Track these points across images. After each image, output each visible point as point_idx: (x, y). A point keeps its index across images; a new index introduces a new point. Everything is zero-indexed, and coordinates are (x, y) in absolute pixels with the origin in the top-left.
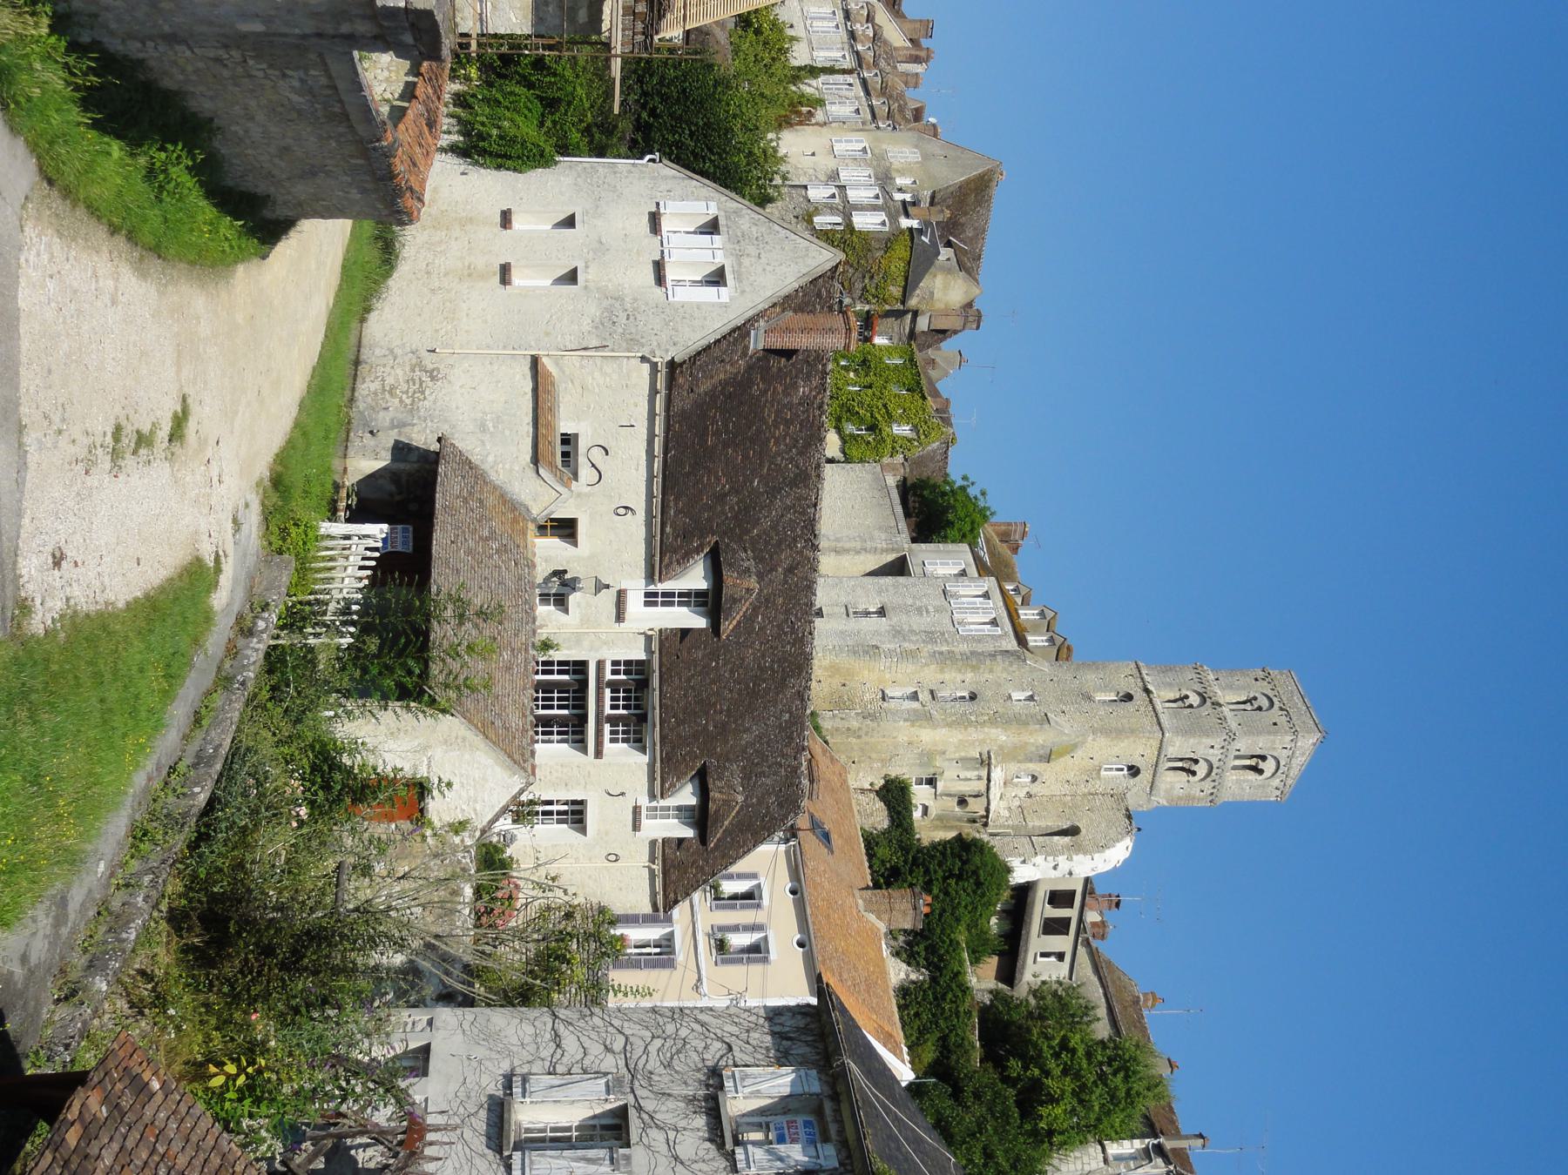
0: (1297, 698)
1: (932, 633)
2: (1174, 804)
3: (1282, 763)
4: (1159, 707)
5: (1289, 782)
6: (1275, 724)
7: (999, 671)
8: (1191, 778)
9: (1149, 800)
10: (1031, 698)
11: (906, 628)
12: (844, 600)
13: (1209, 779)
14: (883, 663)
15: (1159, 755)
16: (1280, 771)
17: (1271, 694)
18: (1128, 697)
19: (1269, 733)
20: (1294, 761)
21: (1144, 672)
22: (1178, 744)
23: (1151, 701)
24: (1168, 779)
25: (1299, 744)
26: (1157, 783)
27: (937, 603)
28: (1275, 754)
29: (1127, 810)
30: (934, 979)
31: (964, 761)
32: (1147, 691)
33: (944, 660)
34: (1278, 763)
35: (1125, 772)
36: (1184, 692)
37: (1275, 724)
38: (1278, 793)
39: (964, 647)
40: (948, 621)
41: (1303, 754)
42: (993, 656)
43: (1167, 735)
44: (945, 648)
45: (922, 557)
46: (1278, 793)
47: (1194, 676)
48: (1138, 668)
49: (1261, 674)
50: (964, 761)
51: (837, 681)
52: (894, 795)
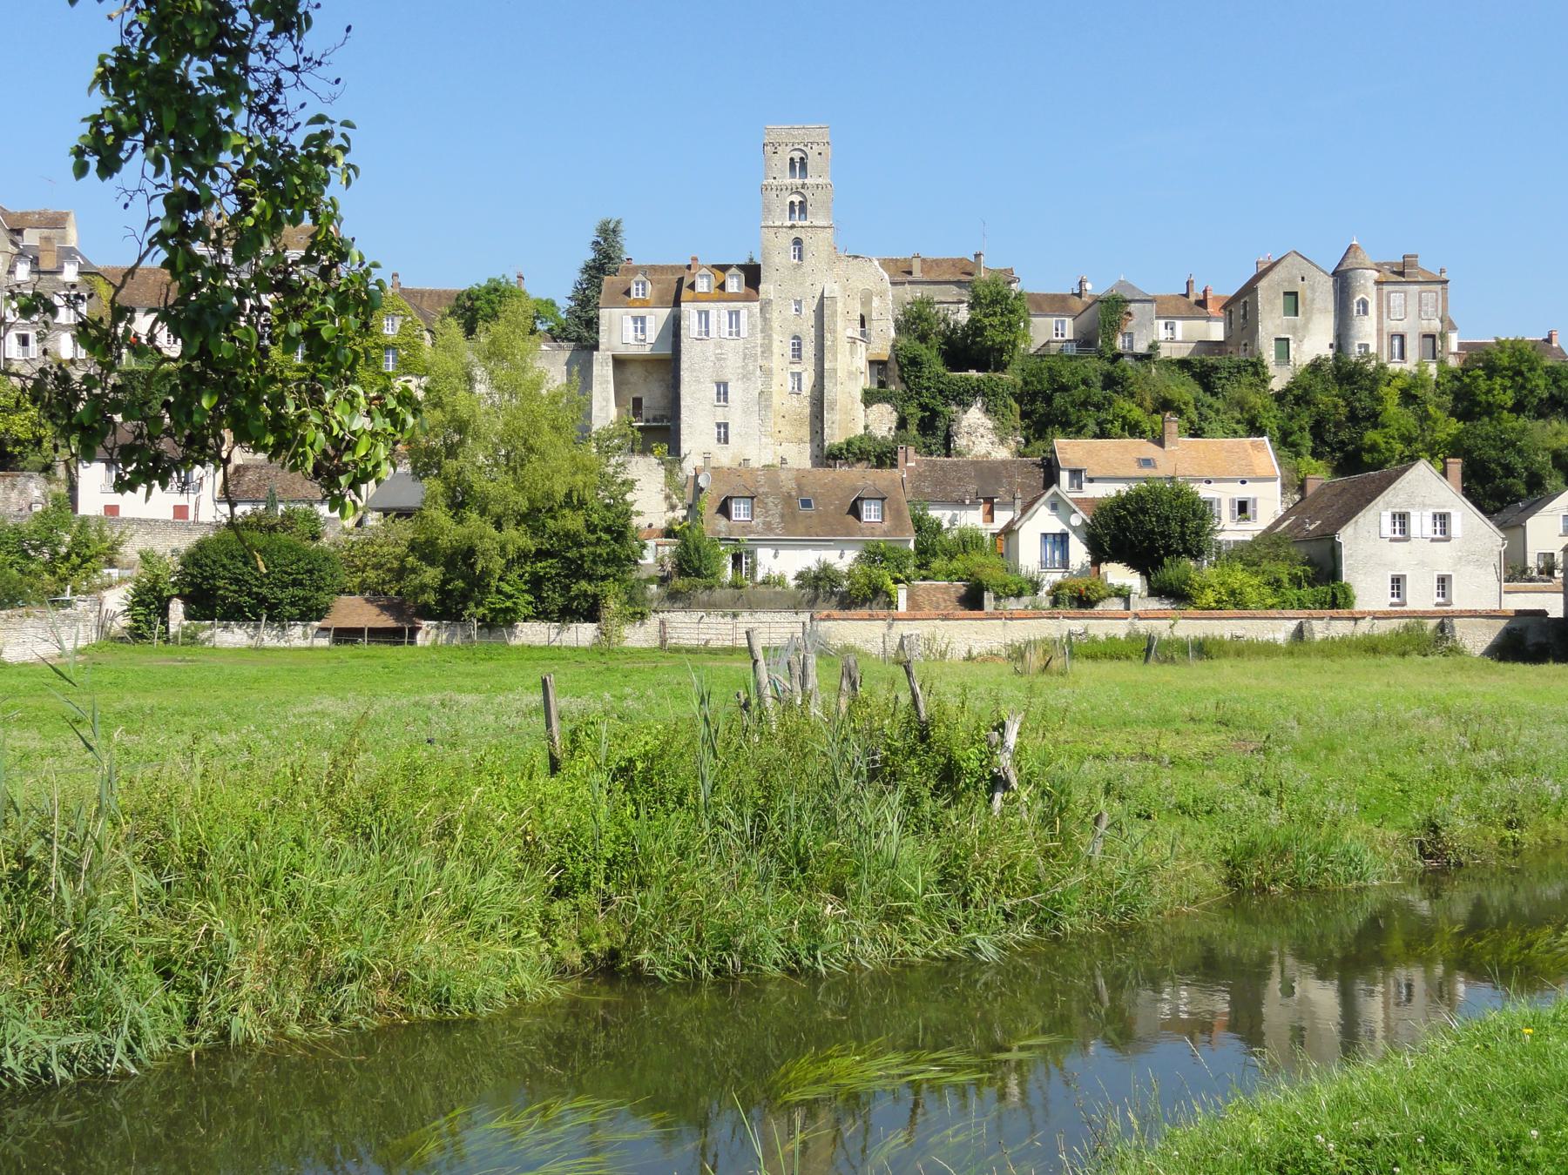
1: (745, 355)
4: (807, 223)
7: (775, 316)
10: (798, 303)
11: (740, 371)
12: (708, 407)
14: (775, 388)
17: (790, 148)
18: (798, 242)
21: (771, 224)
27: (712, 347)
30: (984, 395)
31: (852, 353)
32: (792, 227)
33: (767, 350)
39: (759, 336)
40: (732, 343)
42: (765, 320)
44: (759, 350)
45: (616, 341)
47: (774, 192)
50: (852, 353)
51: (780, 420)
52: (869, 399)
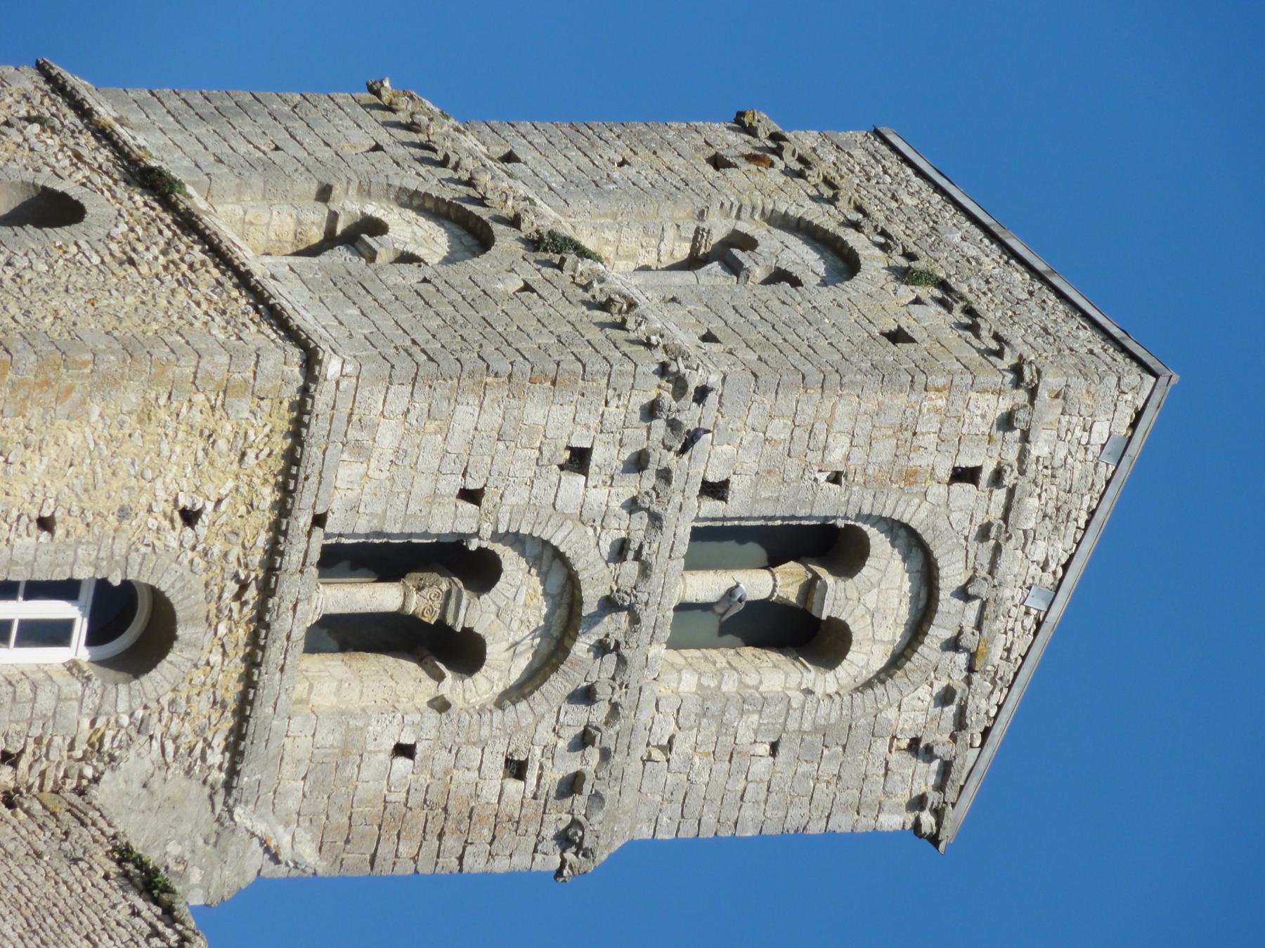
0: (956, 232)
2: (356, 860)
3: (951, 574)
5: (981, 705)
6: (898, 336)
8: (451, 685)
9: (224, 823)
13: (559, 685)
15: (283, 509)
16: (939, 632)
17: (824, 217)
19: (884, 376)
20: (1011, 562)
22: (387, 436)
23: (189, 223)
24: (325, 697)
25: (1039, 448)
26: (262, 712)
28: (915, 514)
29: (124, 855)
34: (927, 576)
35: (78, 649)
36: (350, 207)
37: (898, 336)
38: (923, 777)
41: (1057, 516)
43: (332, 367)
46: (923, 777)
48: (58, 87)
49: (733, 143)
